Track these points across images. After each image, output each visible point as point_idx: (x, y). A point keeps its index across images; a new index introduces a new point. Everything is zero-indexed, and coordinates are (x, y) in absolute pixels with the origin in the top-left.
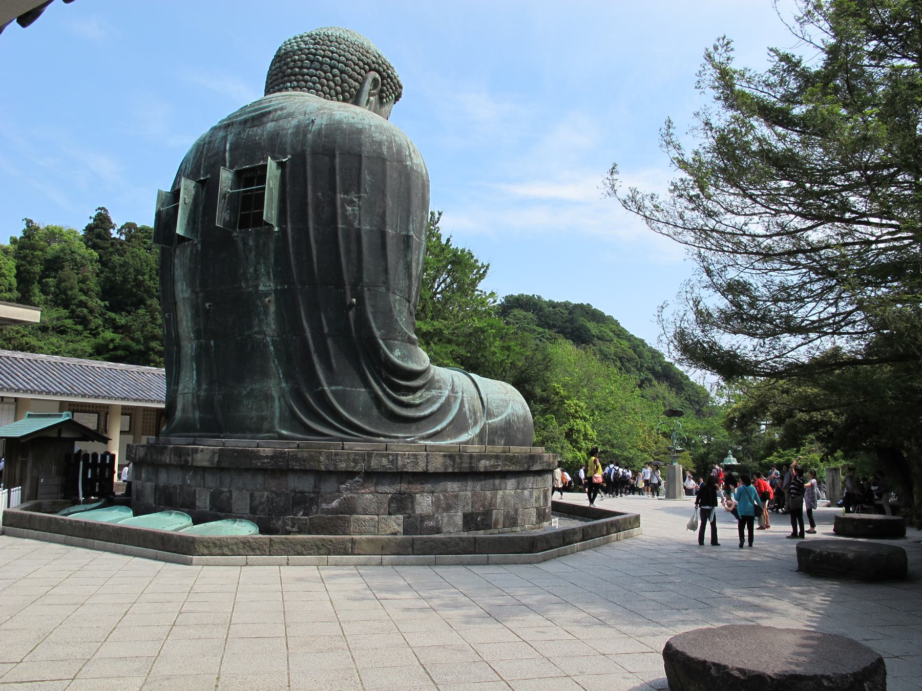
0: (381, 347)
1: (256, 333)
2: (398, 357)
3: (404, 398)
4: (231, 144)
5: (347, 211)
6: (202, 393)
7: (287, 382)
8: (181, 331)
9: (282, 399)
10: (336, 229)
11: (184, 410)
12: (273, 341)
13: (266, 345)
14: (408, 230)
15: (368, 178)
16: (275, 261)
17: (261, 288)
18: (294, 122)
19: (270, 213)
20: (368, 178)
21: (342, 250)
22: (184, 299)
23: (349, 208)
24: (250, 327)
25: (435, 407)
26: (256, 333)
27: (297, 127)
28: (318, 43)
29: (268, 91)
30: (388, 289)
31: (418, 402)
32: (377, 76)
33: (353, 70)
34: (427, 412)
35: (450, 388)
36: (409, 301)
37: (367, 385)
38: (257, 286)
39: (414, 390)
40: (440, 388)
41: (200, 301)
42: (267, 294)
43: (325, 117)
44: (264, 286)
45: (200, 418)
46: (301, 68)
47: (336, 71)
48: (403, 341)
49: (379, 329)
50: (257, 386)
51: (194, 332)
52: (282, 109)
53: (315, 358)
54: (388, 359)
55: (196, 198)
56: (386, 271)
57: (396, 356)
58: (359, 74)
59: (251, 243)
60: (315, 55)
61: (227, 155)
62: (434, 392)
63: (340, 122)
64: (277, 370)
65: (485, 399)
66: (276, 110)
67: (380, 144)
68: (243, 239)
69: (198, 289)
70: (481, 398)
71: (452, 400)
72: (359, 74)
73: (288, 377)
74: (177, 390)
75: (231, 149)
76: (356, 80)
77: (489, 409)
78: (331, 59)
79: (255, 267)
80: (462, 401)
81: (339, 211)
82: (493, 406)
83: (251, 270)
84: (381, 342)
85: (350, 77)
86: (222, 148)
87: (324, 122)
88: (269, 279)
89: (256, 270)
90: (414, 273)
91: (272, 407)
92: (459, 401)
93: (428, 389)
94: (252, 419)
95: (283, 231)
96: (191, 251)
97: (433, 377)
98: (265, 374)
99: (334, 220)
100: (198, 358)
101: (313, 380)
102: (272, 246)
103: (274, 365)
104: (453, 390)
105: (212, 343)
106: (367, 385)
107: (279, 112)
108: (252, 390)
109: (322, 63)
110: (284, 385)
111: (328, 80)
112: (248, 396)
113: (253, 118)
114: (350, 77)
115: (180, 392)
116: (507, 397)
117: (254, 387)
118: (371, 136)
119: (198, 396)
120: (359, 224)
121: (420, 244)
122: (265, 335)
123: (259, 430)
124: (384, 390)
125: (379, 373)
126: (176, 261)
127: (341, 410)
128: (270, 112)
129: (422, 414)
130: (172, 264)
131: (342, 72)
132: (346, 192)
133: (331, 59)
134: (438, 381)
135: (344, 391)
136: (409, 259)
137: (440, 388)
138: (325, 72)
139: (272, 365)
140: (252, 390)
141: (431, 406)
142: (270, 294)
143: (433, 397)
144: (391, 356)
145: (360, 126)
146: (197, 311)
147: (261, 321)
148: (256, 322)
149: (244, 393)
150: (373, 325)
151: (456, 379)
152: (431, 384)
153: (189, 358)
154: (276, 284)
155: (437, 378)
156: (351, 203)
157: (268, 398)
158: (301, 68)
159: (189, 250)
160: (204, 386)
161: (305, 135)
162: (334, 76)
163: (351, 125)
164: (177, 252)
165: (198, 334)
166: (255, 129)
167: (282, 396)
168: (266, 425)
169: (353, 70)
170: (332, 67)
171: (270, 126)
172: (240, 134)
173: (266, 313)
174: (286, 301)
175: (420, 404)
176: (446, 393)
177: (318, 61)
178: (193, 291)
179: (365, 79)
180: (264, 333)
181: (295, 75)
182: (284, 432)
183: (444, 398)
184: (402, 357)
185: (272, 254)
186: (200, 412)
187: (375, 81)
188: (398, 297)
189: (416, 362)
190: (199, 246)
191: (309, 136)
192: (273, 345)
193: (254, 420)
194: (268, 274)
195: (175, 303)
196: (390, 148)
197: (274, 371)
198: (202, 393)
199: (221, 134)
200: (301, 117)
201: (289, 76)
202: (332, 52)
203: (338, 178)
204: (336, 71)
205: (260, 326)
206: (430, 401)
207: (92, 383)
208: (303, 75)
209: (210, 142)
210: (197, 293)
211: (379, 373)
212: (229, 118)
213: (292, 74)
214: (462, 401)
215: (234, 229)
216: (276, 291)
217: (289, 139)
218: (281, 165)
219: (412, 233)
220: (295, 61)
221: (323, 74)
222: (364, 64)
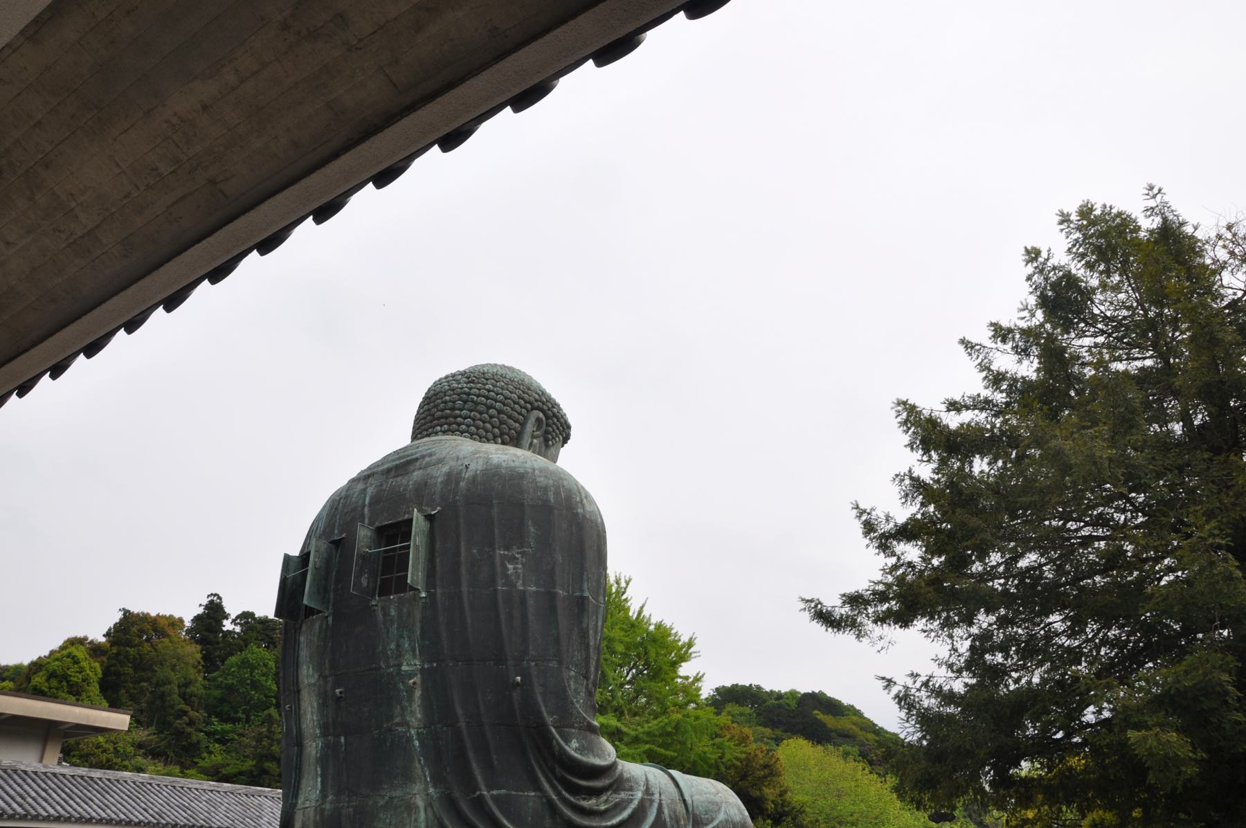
0: (554, 738)
1: (398, 725)
2: (576, 750)
3: (585, 804)
4: (371, 498)
5: (507, 569)
6: (328, 806)
7: (435, 786)
8: (304, 726)
9: (429, 810)
10: (496, 590)
12: (418, 734)
13: (410, 740)
14: (582, 590)
15: (532, 530)
16: (423, 633)
18: (445, 469)
19: (415, 574)
20: (532, 530)
21: (503, 617)
22: (309, 685)
23: (510, 567)
25: (625, 814)
26: (398, 725)
27: (449, 475)
28: (473, 382)
29: (414, 438)
30: (560, 663)
31: (603, 808)
32: (541, 415)
33: (513, 409)
34: (615, 821)
35: (643, 788)
36: (587, 678)
37: (538, 787)
38: (400, 665)
39: (597, 792)
40: (631, 789)
41: (329, 687)
43: (481, 462)
46: (453, 409)
47: (492, 411)
48: (580, 728)
49: (551, 714)
51: (320, 728)
52: (431, 455)
53: (471, 755)
54: (563, 752)
55: (328, 561)
56: (557, 641)
57: (572, 748)
58: (520, 414)
59: (393, 612)
60: (468, 394)
61: (366, 510)
62: (623, 795)
63: (498, 466)
64: (423, 771)
65: (687, 798)
66: (423, 457)
67: (546, 489)
68: (383, 608)
69: (327, 672)
70: (684, 801)
71: (648, 804)
72: (520, 414)
73: (437, 779)
75: (371, 504)
76: (516, 421)
77: (695, 816)
78: (487, 398)
80: (660, 805)
81: (499, 570)
82: (700, 810)
83: (393, 646)
84: (553, 730)
85: (510, 417)
87: (480, 468)
88: (414, 656)
89: (398, 646)
90: (592, 643)
91: (416, 820)
92: (656, 805)
93: (616, 791)
95: (432, 596)
96: (321, 627)
97: (621, 775)
98: (408, 778)
99: (493, 581)
100: (323, 760)
101: (469, 784)
102: (418, 616)
103: (420, 767)
104: (648, 791)
105: (342, 739)
106: (538, 787)
107: (427, 459)
108: (391, 798)
109: (476, 404)
110: (431, 790)
111: (484, 422)
113: (397, 467)
114: (510, 417)
115: (300, 806)
116: (717, 799)
118: (534, 481)
119: (322, 811)
120: (524, 584)
121: (598, 607)
122: (409, 727)
124: (559, 794)
125: (552, 771)
126: (302, 639)
127: (505, 822)
128: (417, 459)
129: (609, 823)
130: (296, 643)
131: (500, 412)
132: (507, 548)
133: (487, 398)
134: (628, 780)
135: (507, 796)
136: (585, 625)
137: (631, 789)
138: (481, 413)
140: (391, 798)
141: (620, 813)
143: (622, 801)
144: (567, 748)
145: (522, 470)
146: (325, 701)
147: (403, 709)
148: (398, 710)
149: (382, 803)
150: (543, 709)
151: (651, 778)
152: (620, 784)
153: (313, 760)
154: (423, 662)
155: (626, 775)
156: (513, 560)
157: (410, 808)
158: (453, 409)
159: (317, 624)
160: (330, 797)
161: (457, 483)
162: (491, 417)
163: (512, 469)
164: (304, 628)
165: (325, 730)
166: (399, 479)
167: (429, 805)
169: (513, 409)
170: (489, 407)
171: (417, 475)
172: (381, 485)
173: (410, 699)
174: (434, 682)
175: (606, 811)
176: (639, 795)
177: (472, 401)
179: (526, 419)
180: (407, 724)
181: (446, 418)
183: (636, 802)
184: (580, 750)
185: (418, 625)
187: (538, 420)
188: (572, 673)
189: (599, 757)
190: (330, 619)
191: (462, 484)
192: (418, 739)
194: (413, 649)
195: (299, 691)
196: (557, 494)
197: (419, 771)
198: (328, 806)
199: (360, 486)
200: (453, 463)
201: (439, 419)
202: (489, 391)
203: (496, 531)
204: (492, 411)
205: (403, 715)
206: (619, 807)
207: (185, 808)
208: (455, 417)
209: (347, 497)
210: (325, 677)
211: (552, 771)
212: (370, 468)
213: (442, 417)
214: (660, 805)
215: (373, 596)
216: (422, 671)
217: (438, 488)
218: (429, 518)
219: (586, 594)
220: (446, 402)
221: (478, 416)
222: (526, 402)
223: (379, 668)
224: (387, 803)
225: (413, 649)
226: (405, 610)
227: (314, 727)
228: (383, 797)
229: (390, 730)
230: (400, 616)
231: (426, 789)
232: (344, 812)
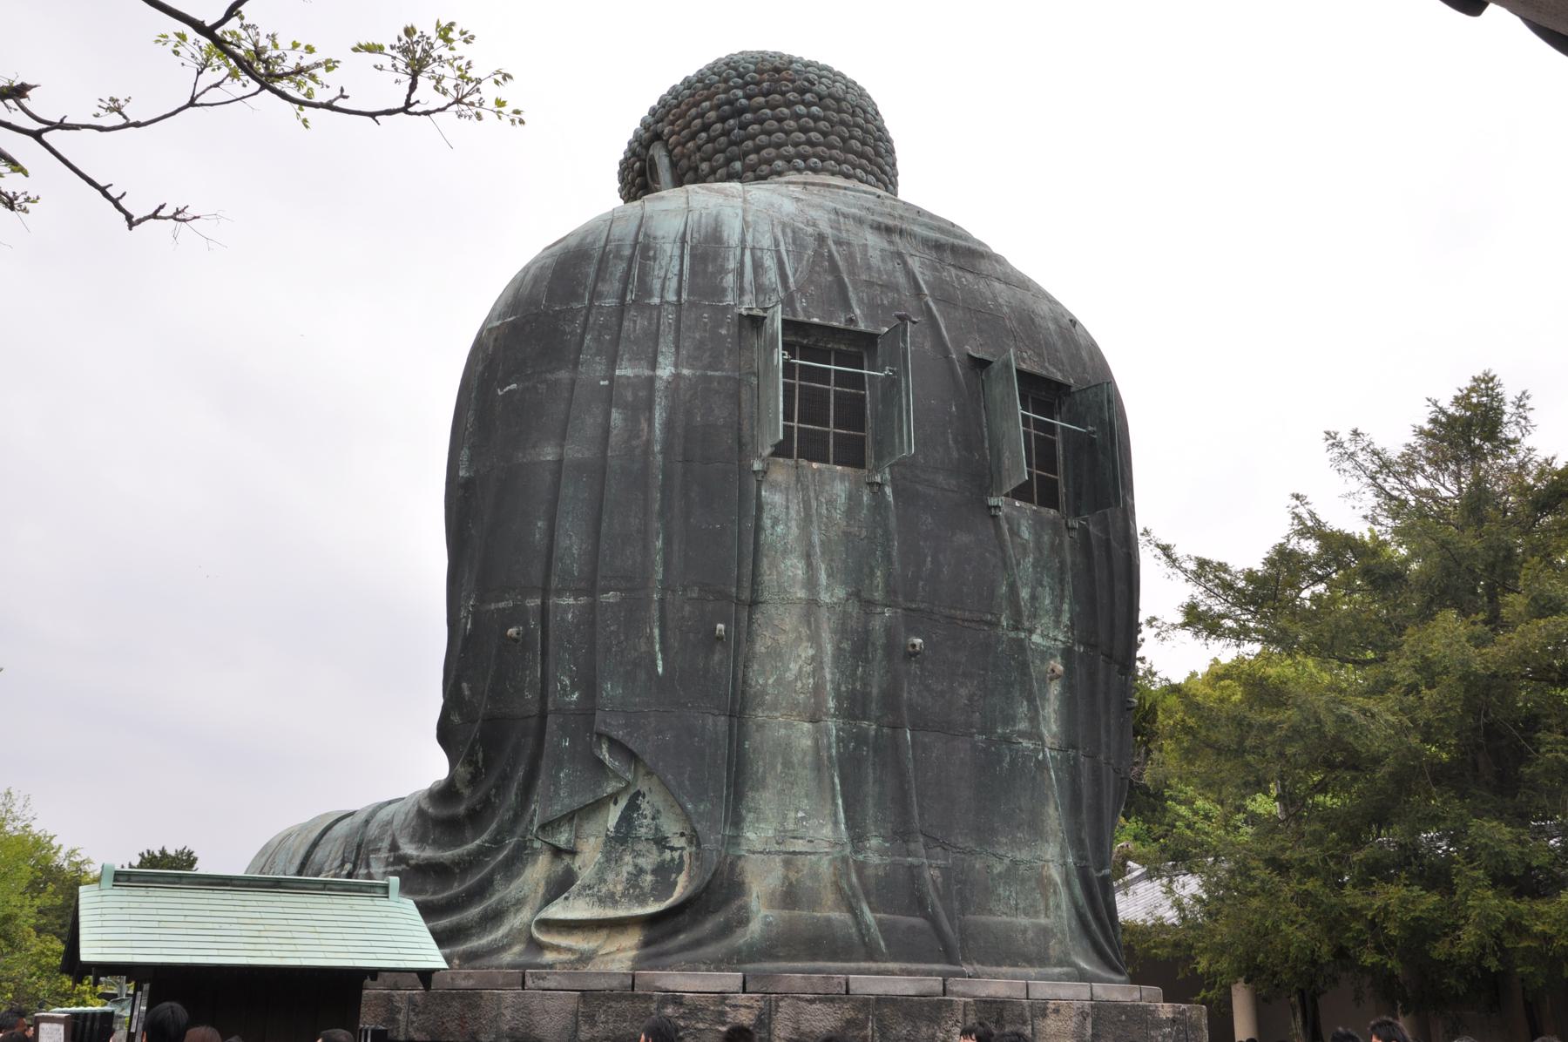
6: (874, 859)
11: (790, 896)
17: (1036, 638)
24: (1010, 719)
26: (1022, 734)
38: (1031, 631)
41: (877, 624)
42: (1045, 655)
44: (1043, 636)
45: (880, 923)
50: (1023, 855)
51: (838, 696)
68: (1007, 518)
69: (878, 596)
74: (735, 840)
79: (1034, 589)
86: (901, 279)
88: (1057, 622)
89: (1033, 597)
91: (1058, 907)
94: (1024, 931)
96: (853, 498)
98: (1036, 830)
103: (1053, 816)
108: (1015, 862)
112: (1010, 875)
117: (1019, 857)
119: (861, 867)
122: (1043, 744)
123: (1042, 960)
139: (1051, 810)
142: (1053, 656)
146: (856, 648)
149: (999, 868)
159: (840, 490)
160: (874, 842)
168: (1055, 949)
173: (1044, 698)
178: (857, 594)
180: (1041, 738)
182: (1083, 965)
186: (873, 910)
190: (888, 490)
193: (1030, 934)
194: (1058, 612)
195: (754, 603)
210: (867, 605)
223: (998, 624)
224: (1008, 870)
225: (1058, 612)
226: (1046, 538)
227: (818, 690)
228: (1000, 858)
229: (1007, 740)
230: (1039, 548)
231: (1064, 856)
232: (927, 875)
